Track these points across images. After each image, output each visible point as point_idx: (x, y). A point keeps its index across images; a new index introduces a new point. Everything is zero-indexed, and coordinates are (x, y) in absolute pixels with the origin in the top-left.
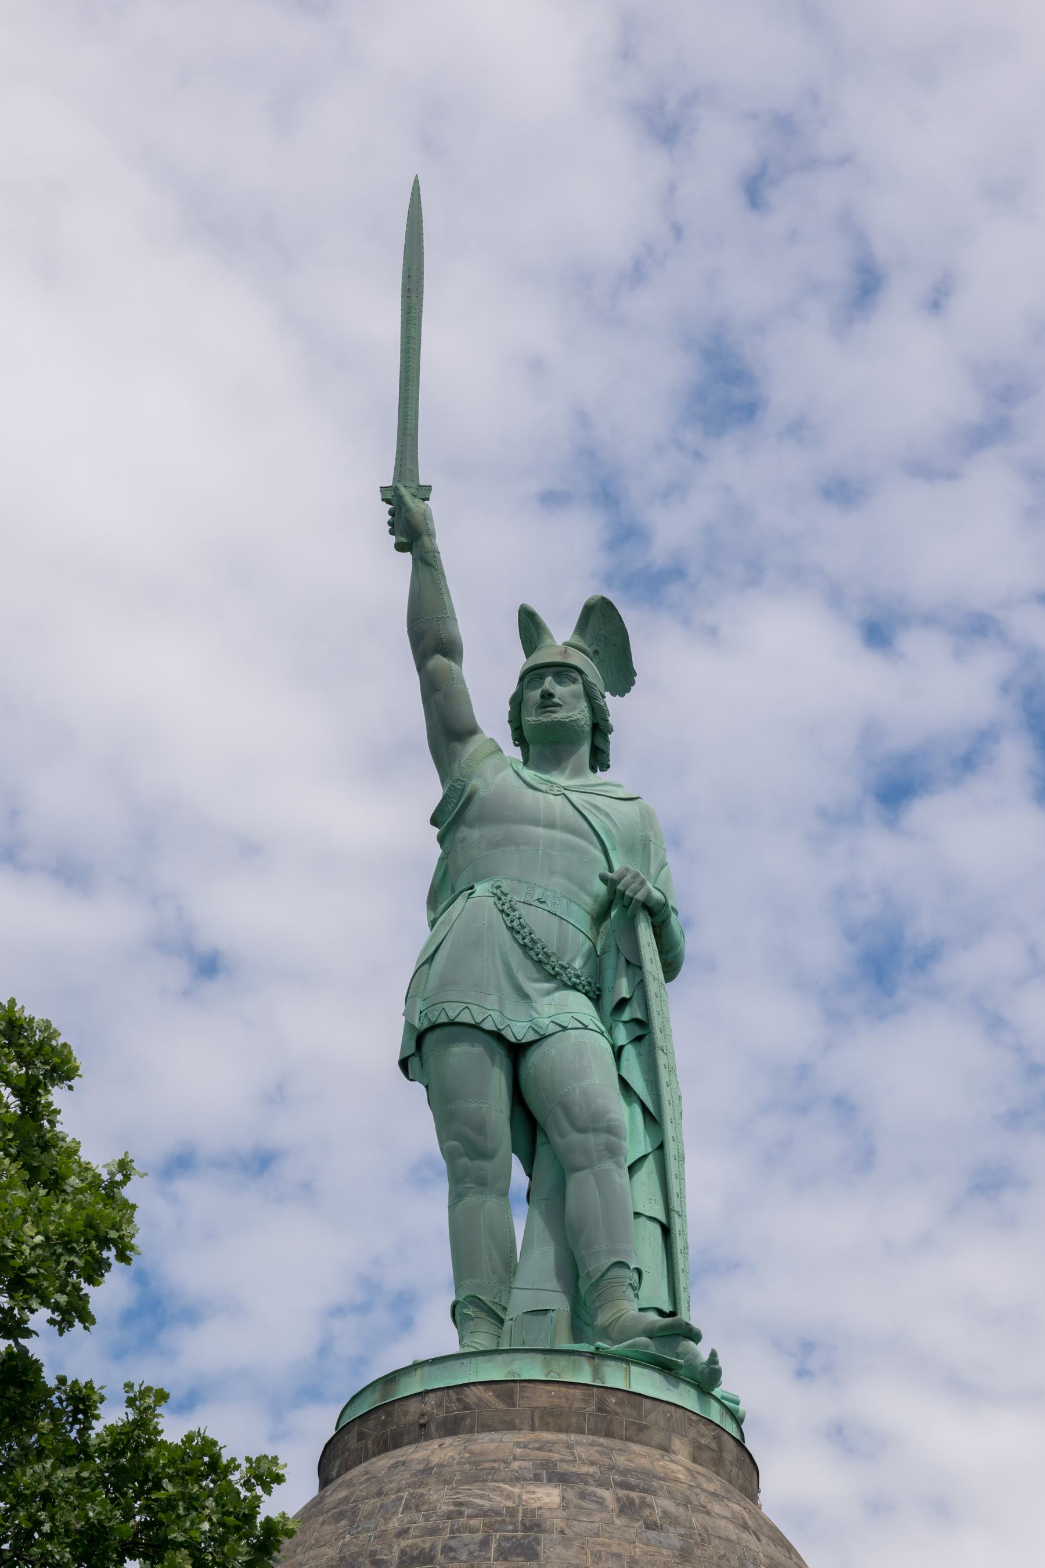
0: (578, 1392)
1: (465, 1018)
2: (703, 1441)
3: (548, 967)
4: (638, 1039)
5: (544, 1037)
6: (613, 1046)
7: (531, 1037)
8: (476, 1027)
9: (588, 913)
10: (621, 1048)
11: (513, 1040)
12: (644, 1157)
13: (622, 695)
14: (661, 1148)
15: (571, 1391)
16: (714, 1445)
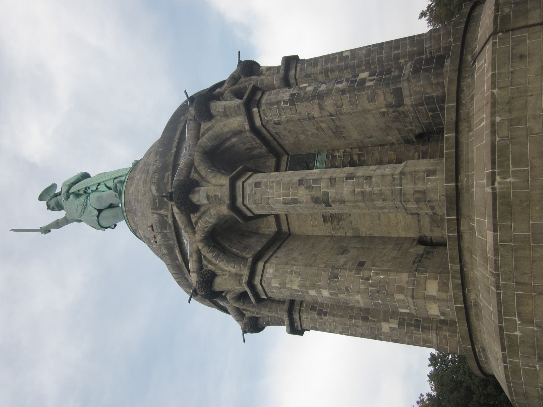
0: (128, 217)
1: (97, 223)
2: (130, 184)
3: (85, 207)
4: (89, 188)
5: (94, 208)
6: (92, 192)
7: (95, 210)
8: (98, 221)
9: (76, 199)
10: (92, 191)
11: (98, 213)
12: (105, 185)
13: (57, 185)
14: (103, 182)
15: (129, 218)
16: (131, 180)
